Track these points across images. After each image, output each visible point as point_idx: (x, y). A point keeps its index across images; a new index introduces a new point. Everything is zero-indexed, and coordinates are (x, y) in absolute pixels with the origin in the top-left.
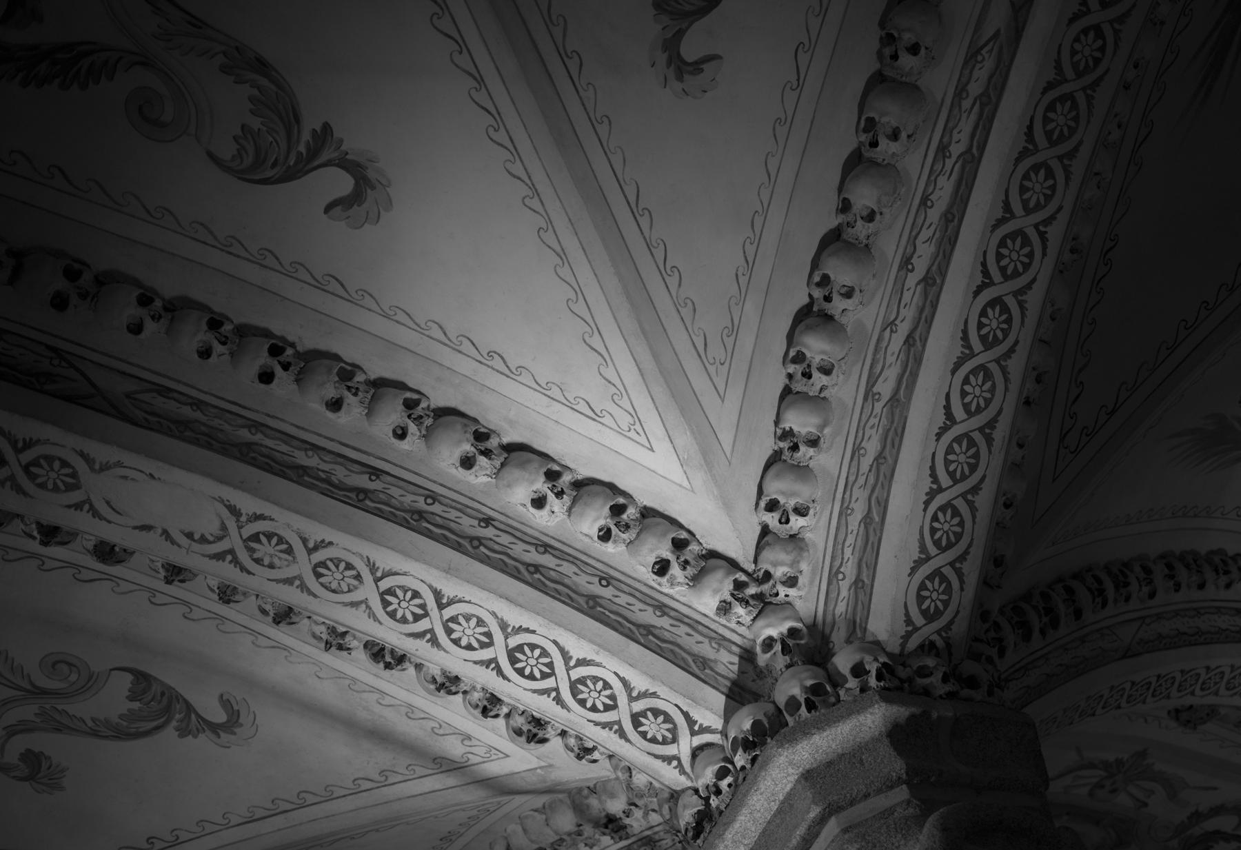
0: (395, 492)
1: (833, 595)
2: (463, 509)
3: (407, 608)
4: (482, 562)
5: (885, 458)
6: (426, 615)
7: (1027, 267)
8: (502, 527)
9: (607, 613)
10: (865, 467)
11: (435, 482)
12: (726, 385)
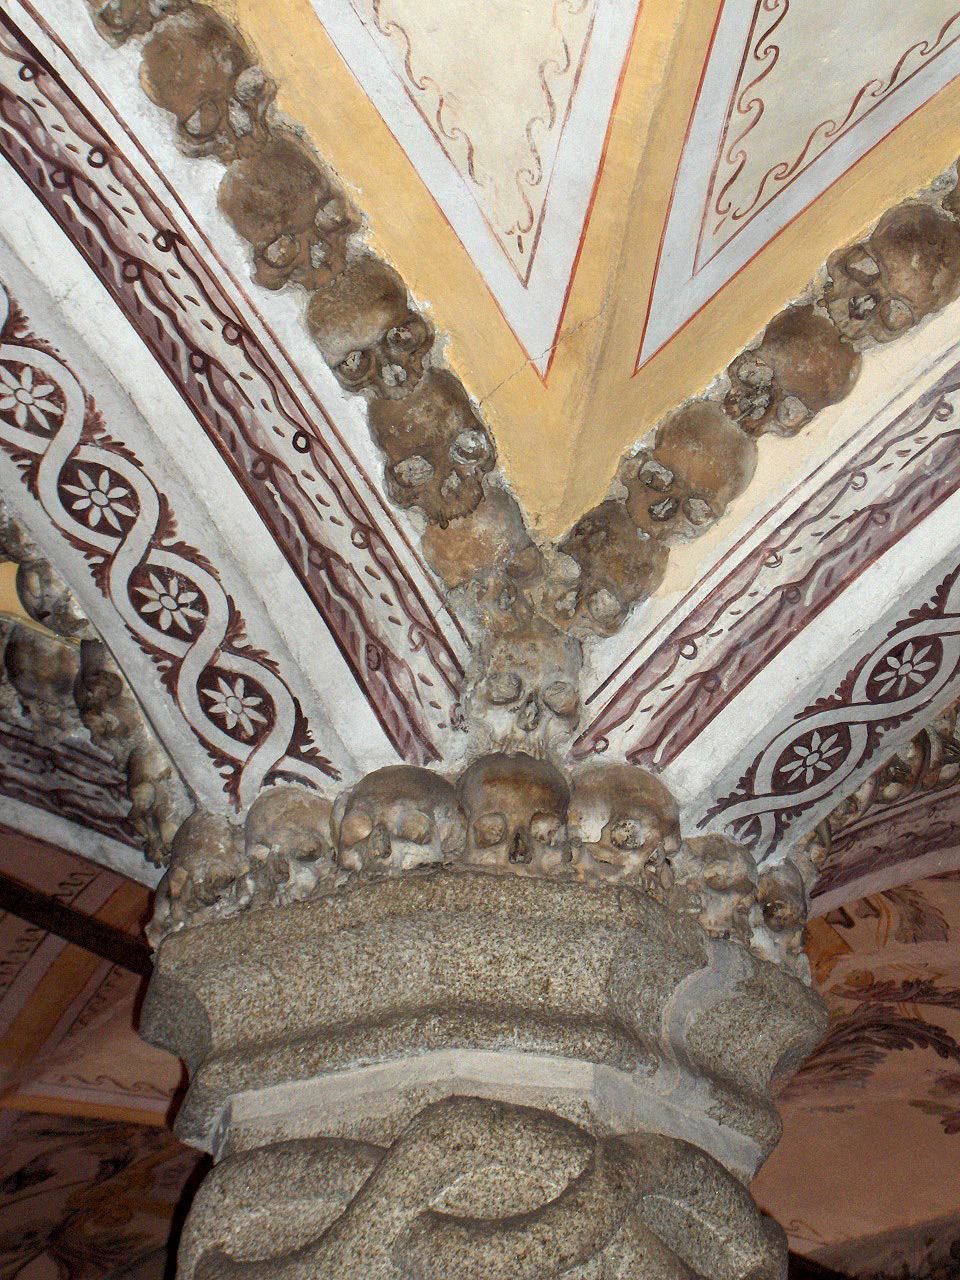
0: (50, 115)
1: (657, 670)
4: (124, 308)
5: (888, 516)
8: (190, 260)
9: (277, 497)
10: (845, 508)
11: (124, 126)
12: (718, 252)
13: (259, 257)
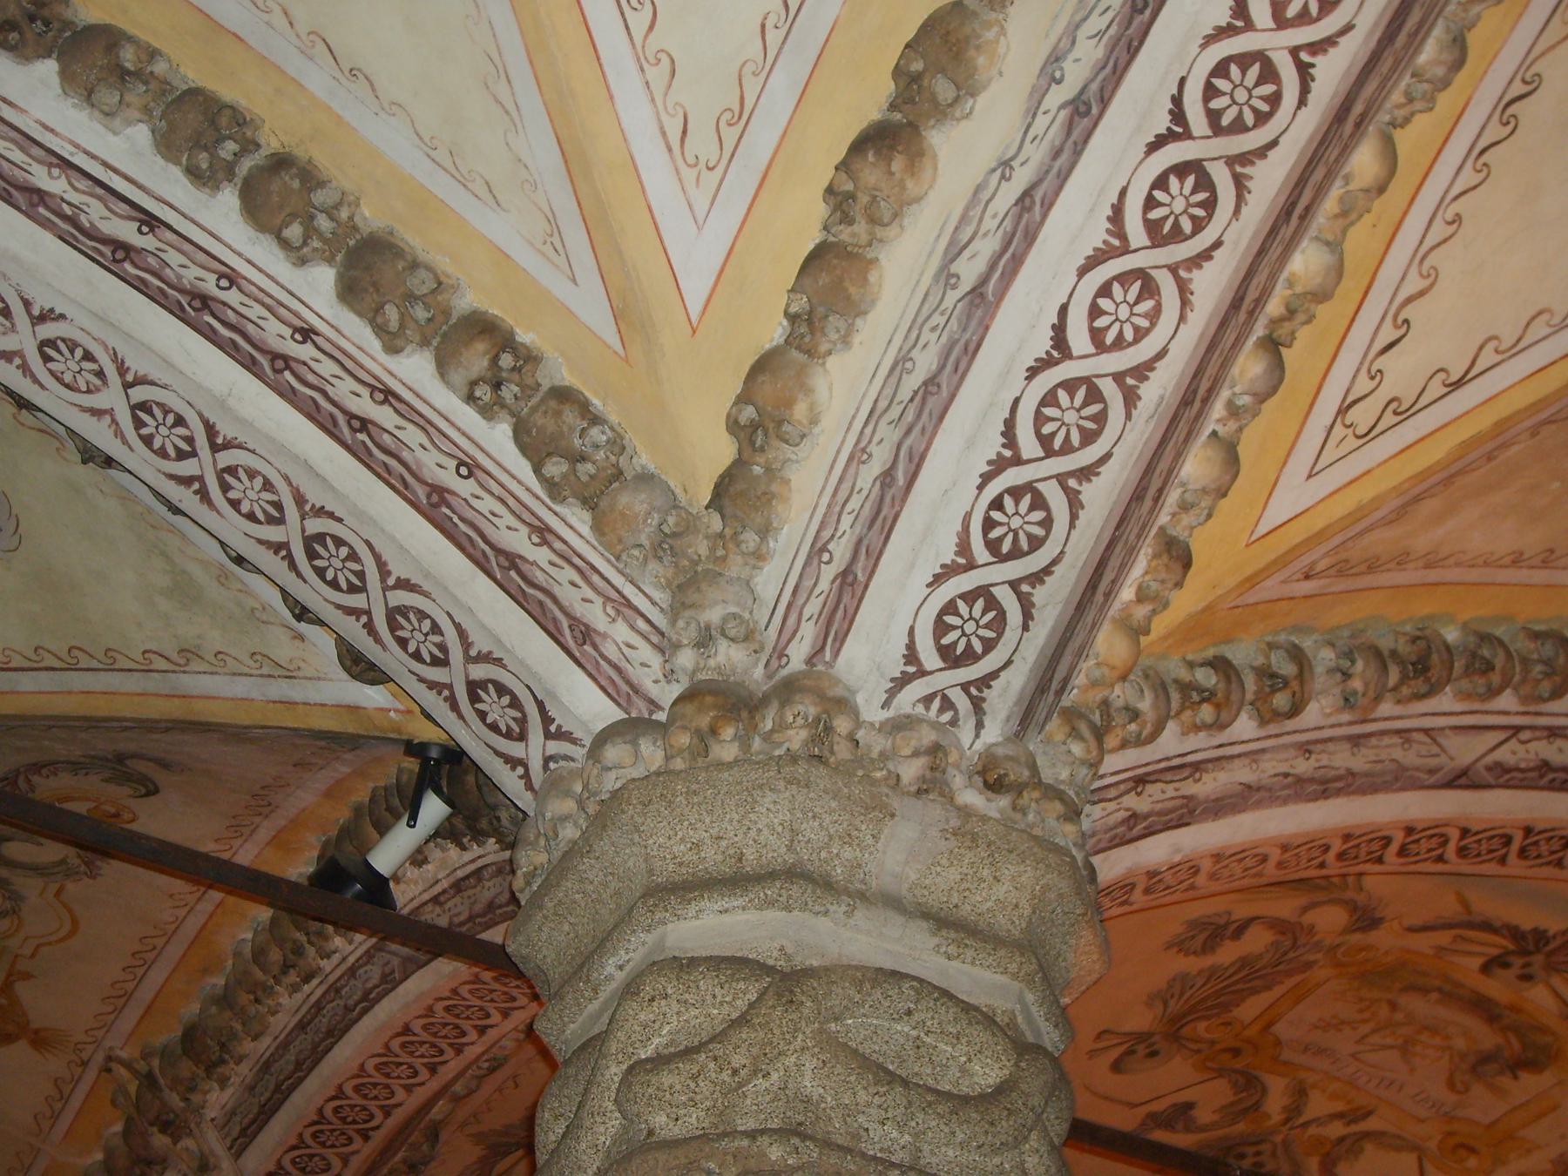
0: (173, 258)
1: (808, 583)
2: (273, 308)
3: (170, 438)
4: (281, 395)
5: (939, 386)
6: (194, 454)
7: (1262, 118)
9: (456, 519)
10: (905, 394)
11: (240, 255)
12: (712, 204)
13: (380, 330)
